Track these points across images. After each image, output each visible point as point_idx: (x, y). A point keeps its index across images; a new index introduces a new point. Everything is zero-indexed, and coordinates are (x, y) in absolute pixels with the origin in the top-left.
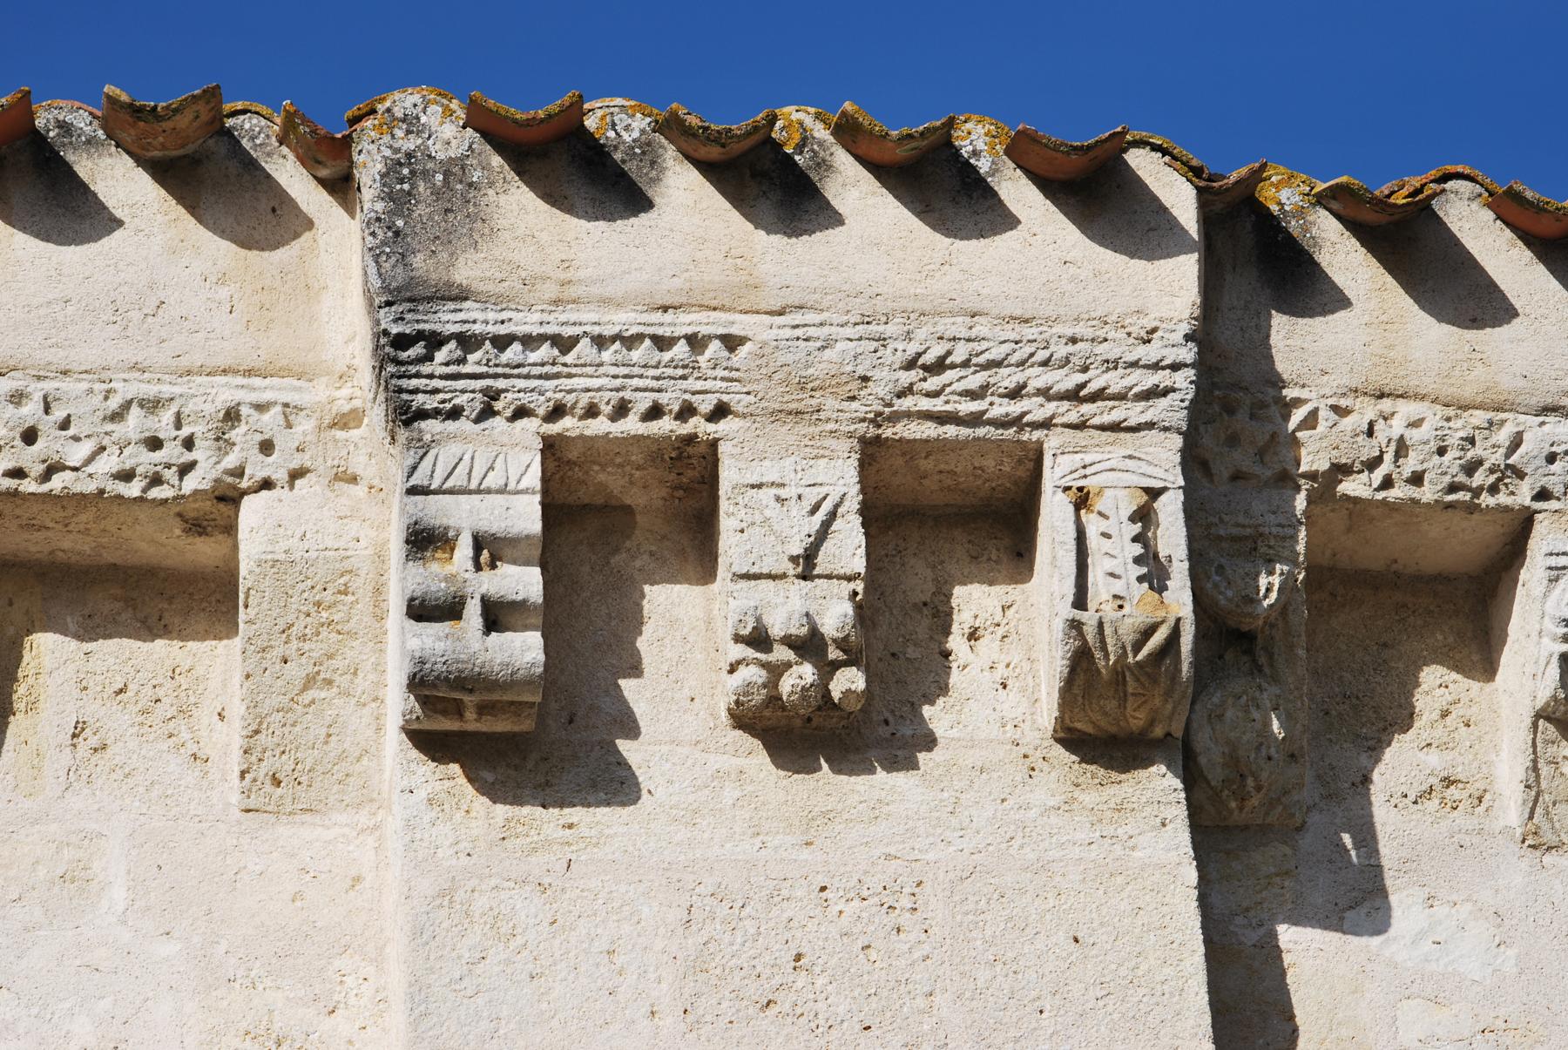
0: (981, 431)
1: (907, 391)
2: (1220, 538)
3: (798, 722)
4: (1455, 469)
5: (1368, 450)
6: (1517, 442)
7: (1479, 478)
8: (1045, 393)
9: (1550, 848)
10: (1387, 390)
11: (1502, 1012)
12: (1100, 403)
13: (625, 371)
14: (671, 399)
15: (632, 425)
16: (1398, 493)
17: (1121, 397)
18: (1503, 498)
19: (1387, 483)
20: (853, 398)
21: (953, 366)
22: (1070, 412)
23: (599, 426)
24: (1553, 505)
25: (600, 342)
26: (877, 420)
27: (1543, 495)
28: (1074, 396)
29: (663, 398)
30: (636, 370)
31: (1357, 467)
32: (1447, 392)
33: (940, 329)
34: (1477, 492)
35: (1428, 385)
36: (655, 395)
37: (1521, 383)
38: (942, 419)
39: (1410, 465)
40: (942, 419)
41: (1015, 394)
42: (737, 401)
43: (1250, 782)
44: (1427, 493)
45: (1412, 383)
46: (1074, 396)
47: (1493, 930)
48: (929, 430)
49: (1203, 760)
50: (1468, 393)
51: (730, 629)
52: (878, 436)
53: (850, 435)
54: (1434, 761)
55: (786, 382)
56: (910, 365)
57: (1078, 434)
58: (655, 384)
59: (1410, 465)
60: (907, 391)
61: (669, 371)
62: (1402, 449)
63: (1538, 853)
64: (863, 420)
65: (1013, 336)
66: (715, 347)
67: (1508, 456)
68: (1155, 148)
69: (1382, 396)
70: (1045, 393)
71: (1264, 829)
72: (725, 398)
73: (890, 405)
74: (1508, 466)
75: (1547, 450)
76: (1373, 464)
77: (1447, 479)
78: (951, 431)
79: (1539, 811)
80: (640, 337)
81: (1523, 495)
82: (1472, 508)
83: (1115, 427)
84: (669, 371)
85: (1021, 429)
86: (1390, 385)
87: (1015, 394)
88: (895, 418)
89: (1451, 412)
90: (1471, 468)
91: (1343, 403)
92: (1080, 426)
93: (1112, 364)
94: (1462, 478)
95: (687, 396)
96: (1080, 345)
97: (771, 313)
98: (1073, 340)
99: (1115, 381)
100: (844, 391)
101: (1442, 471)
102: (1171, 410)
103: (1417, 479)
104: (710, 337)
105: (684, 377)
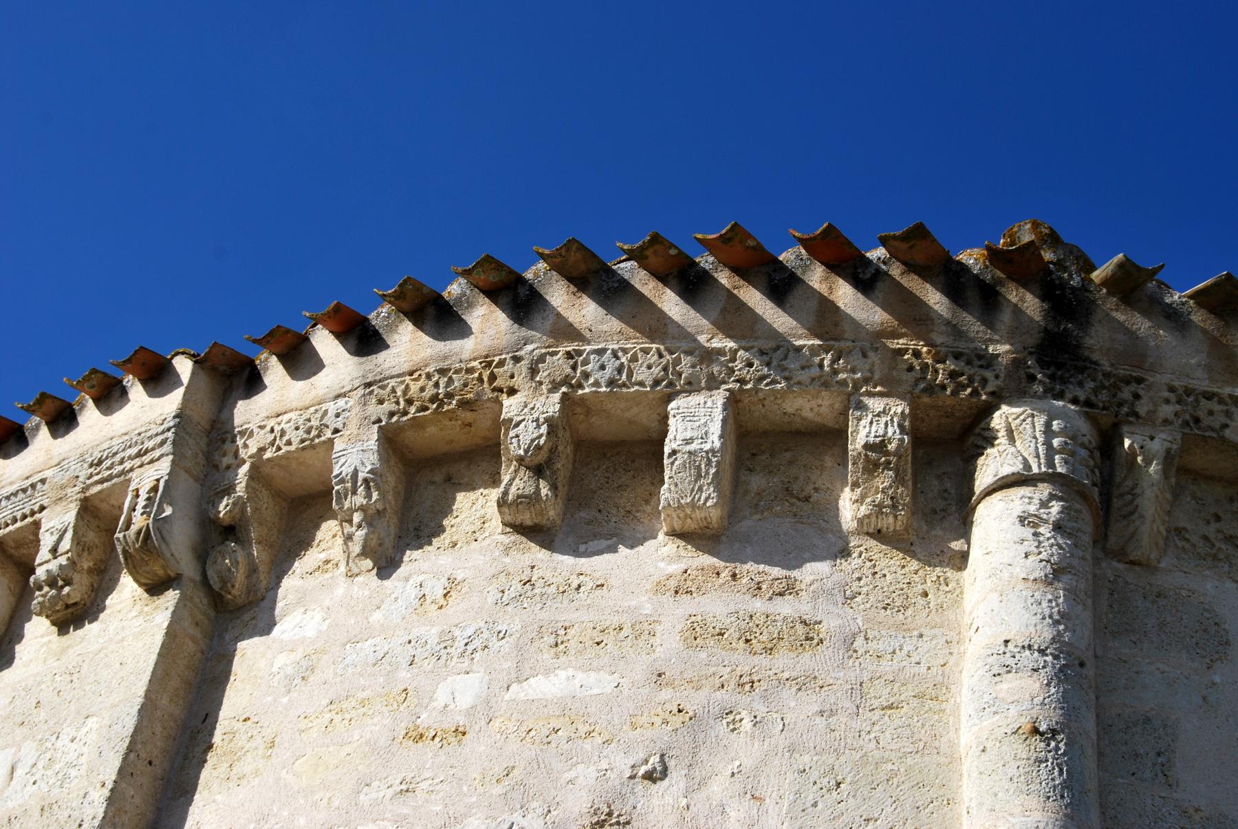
0: (113, 481)
1: (91, 476)
2: (218, 493)
3: (69, 615)
4: (302, 433)
5: (271, 437)
6: (326, 412)
7: (314, 433)
8: (131, 458)
9: (357, 575)
10: (279, 413)
11: (315, 647)
12: (148, 454)
13: (14, 505)
14: (27, 511)
15: (19, 524)
16: (285, 449)
17: (153, 449)
18: (323, 438)
19: (279, 449)
20: (75, 486)
21: (104, 460)
22: (137, 462)
23: (11, 528)
24: (341, 433)
25: (8, 498)
26: (84, 490)
27: (336, 431)
28: (139, 455)
29: (24, 511)
30: (18, 504)
31: (267, 446)
32: (300, 404)
33: (99, 449)
34: (312, 440)
35: (294, 405)
36: (21, 511)
37: (327, 390)
38: (101, 481)
39: (285, 439)
40: (101, 481)
41: (122, 462)
42: (45, 502)
43: (229, 585)
44: (292, 448)
45: (289, 406)
46: (139, 455)
47: (324, 615)
48: (98, 488)
49: (211, 582)
50: (307, 403)
51: (157, 602)
52: (85, 497)
53: (76, 500)
54: (323, 556)
55: (57, 489)
56: (91, 465)
57: (142, 469)
58: (21, 507)
59: (285, 439)
60: (91, 476)
61: (26, 500)
62: (283, 433)
63: (352, 579)
64: (79, 492)
65: (122, 441)
66: (39, 486)
67: (321, 421)
68: (183, 353)
69: (278, 416)
70: (131, 458)
71: (251, 603)
72: (41, 503)
73: (85, 483)
74: (321, 425)
75: (335, 412)
76: (272, 443)
77: (299, 438)
78: (105, 485)
79: (350, 561)
80: (17, 491)
81: (328, 434)
82: (313, 447)
83: (152, 462)
84: (26, 500)
85: (126, 475)
86: (280, 409)
87: (122, 462)
88: (87, 488)
89: (302, 412)
90: (308, 432)
91: (262, 424)
92: (141, 466)
93: (150, 438)
94: (305, 436)
95: (32, 507)
96: (143, 435)
97: (56, 466)
98: (139, 434)
99: (150, 444)
100: (72, 485)
101: (295, 437)
102: (168, 448)
103: (289, 443)
104: (37, 482)
105: (30, 500)
